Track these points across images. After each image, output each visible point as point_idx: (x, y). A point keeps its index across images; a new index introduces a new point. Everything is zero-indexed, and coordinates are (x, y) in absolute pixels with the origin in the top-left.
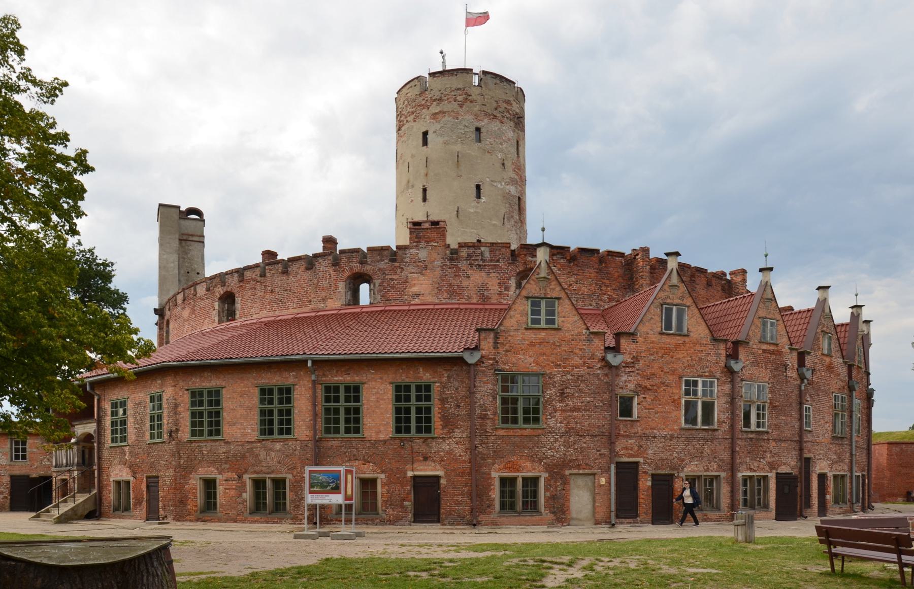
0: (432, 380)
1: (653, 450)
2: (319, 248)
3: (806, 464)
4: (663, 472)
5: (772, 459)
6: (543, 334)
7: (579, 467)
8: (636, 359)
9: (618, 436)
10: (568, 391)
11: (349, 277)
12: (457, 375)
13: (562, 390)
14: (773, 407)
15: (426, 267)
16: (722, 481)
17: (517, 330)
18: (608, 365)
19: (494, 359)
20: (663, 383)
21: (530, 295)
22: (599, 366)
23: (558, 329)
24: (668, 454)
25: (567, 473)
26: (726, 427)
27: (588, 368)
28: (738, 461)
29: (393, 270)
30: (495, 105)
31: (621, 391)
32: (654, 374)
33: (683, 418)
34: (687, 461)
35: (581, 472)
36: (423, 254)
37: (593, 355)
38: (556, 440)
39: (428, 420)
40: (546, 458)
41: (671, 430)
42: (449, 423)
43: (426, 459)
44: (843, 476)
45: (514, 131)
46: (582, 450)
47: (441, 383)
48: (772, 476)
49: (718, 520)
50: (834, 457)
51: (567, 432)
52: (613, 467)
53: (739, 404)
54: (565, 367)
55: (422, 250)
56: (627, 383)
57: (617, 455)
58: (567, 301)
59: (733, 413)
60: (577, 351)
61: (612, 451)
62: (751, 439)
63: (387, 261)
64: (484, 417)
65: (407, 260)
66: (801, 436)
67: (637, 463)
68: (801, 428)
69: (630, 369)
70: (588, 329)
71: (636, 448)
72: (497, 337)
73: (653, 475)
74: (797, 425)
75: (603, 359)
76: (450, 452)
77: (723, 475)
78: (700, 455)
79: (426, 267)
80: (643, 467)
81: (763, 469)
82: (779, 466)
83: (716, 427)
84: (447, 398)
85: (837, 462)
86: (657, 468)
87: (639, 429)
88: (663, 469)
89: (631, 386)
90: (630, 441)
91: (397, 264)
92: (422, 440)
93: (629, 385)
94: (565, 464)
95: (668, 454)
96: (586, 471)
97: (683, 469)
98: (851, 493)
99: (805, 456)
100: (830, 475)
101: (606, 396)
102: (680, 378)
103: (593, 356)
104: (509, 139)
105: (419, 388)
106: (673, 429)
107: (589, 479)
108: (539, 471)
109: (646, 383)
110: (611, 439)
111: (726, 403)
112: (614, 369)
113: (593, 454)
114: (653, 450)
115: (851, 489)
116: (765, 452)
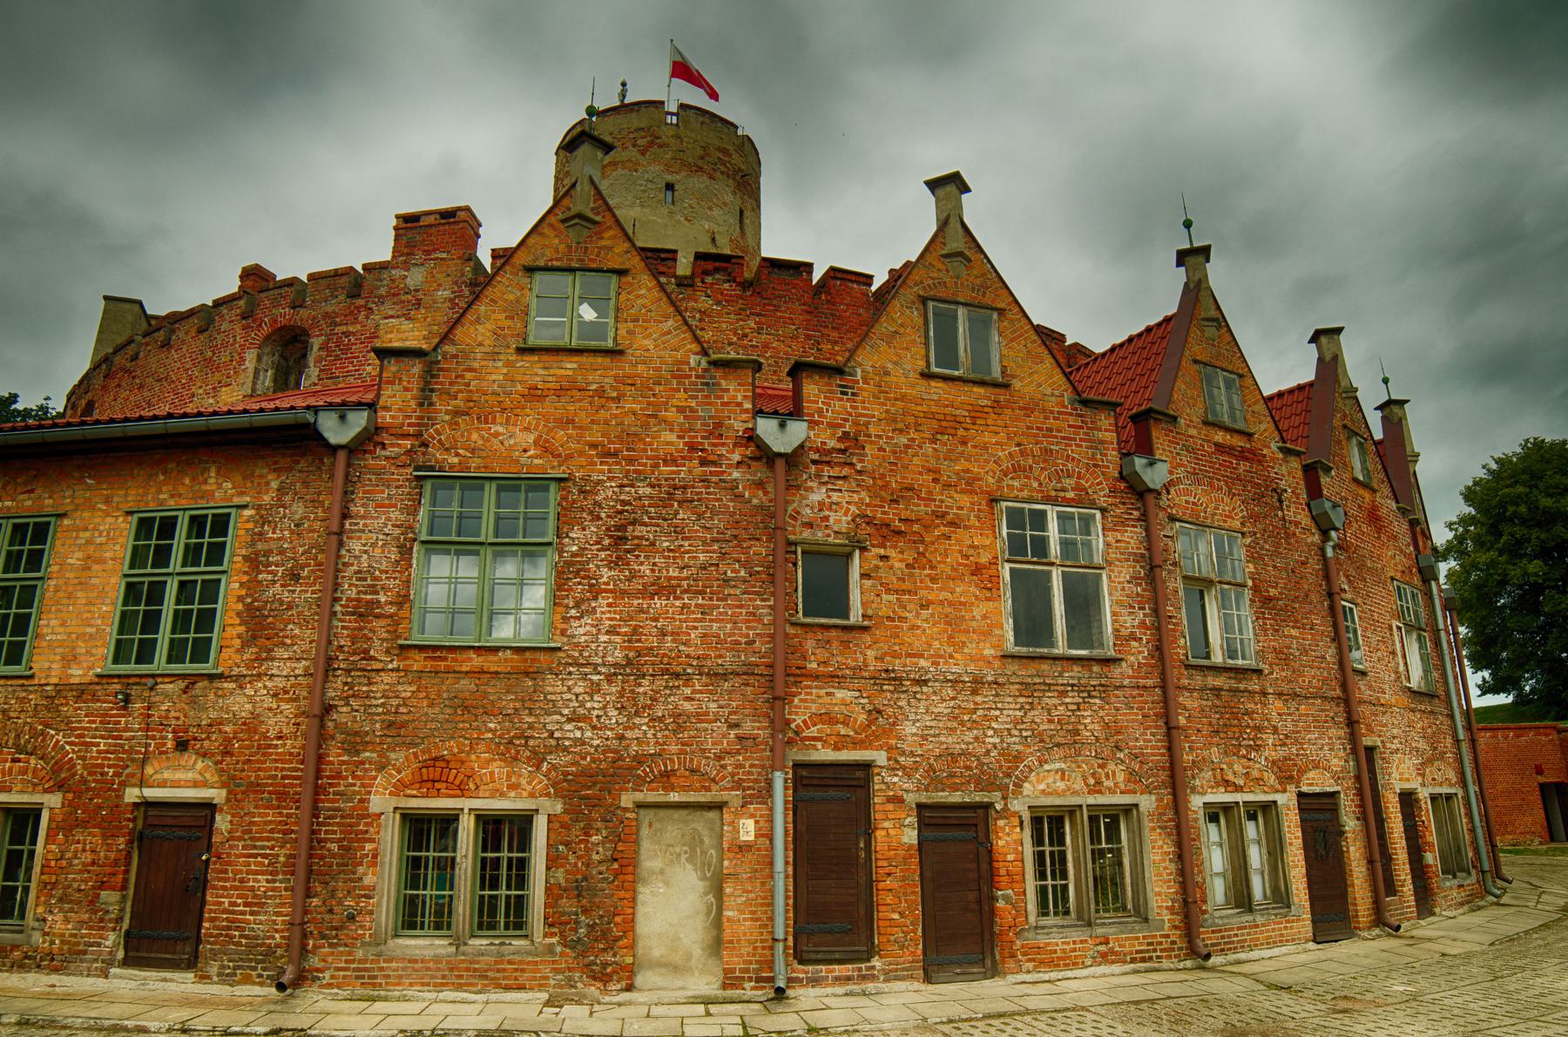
0: (237, 501)
1: (921, 723)
2: (233, 286)
3: (1366, 761)
4: (956, 798)
5: (1282, 752)
6: (570, 365)
7: (666, 779)
8: (852, 442)
9: (799, 675)
10: (640, 530)
11: (267, 338)
12: (306, 484)
13: (619, 528)
14: (1264, 602)
15: (419, 303)
16: (1147, 824)
17: (493, 355)
18: (765, 455)
19: (418, 435)
20: (943, 515)
21: (541, 263)
22: (736, 457)
23: (615, 353)
24: (969, 736)
25: (627, 800)
26: (1139, 653)
27: (704, 462)
28: (1188, 758)
29: (352, 315)
30: (700, 152)
31: (807, 534)
32: (910, 489)
33: (1009, 626)
34: (1032, 760)
35: (674, 797)
36: (415, 277)
37: (719, 425)
38: (595, 689)
39: (206, 620)
40: (560, 748)
41: (973, 659)
42: (261, 627)
43: (182, 746)
44: (1449, 797)
45: (734, 194)
46: (679, 721)
47: (259, 507)
48: (1286, 800)
49: (1143, 959)
50: (1422, 745)
51: (629, 663)
52: (779, 779)
53: (1171, 585)
54: (631, 461)
55: (414, 270)
56: (827, 507)
57: (796, 739)
58: (646, 279)
59: (1156, 611)
60: (671, 414)
61: (779, 725)
62: (1217, 691)
63: (342, 297)
64: (364, 611)
65: (383, 291)
66: (1344, 686)
67: (867, 766)
68: (1342, 662)
69: (835, 472)
70: (705, 353)
71: (862, 718)
72: (430, 373)
73: (920, 807)
74: (1331, 654)
75: (751, 437)
76: (251, 726)
77: (1147, 803)
78: (1070, 741)
79: (419, 303)
80: (887, 782)
81: (1259, 781)
82: (1302, 772)
83: (1112, 653)
84: (268, 553)
85: (1430, 761)
86: (935, 782)
87: (869, 654)
88: (955, 788)
89: (840, 521)
90: (840, 694)
91: (360, 302)
92: (181, 684)
93: (833, 517)
94: (618, 769)
95: (969, 736)
96: (692, 797)
97: (1018, 786)
98: (1474, 842)
99: (1367, 741)
100: (1424, 794)
101: (760, 549)
102: (993, 501)
103: (717, 430)
104: (725, 204)
105: (197, 523)
106: (983, 658)
107: (701, 823)
108: (532, 795)
109: (890, 514)
110: (777, 680)
111: (1135, 579)
112: (780, 465)
113: (716, 736)
114: (921, 723)
115: (1472, 830)
116: (1258, 729)
